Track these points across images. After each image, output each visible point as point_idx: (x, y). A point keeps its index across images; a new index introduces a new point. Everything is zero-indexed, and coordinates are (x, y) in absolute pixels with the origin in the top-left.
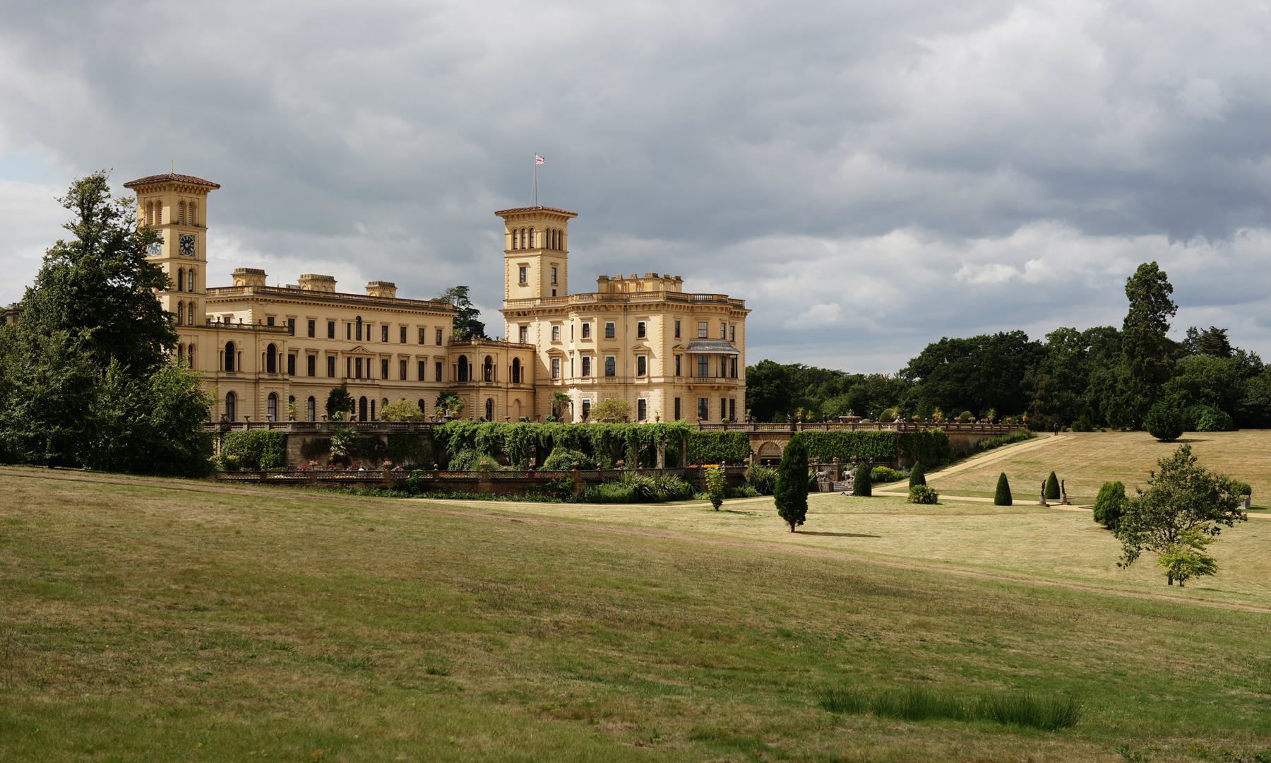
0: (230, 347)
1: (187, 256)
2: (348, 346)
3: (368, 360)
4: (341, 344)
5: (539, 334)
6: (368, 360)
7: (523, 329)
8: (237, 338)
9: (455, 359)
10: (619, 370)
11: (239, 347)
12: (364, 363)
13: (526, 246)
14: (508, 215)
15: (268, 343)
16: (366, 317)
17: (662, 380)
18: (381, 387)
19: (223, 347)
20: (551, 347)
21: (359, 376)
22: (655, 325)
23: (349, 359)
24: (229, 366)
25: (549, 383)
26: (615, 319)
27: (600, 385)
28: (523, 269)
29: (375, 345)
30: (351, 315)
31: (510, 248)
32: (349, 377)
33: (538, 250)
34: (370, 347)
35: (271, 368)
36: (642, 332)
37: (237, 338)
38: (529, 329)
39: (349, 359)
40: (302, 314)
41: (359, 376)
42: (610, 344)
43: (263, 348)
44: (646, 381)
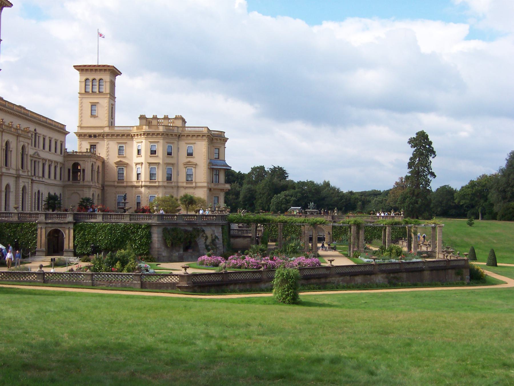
5: (107, 150)
7: (93, 146)
9: (70, 165)
10: (174, 178)
13: (96, 90)
14: (82, 69)
17: (205, 184)
20: (119, 160)
22: (201, 149)
25: (116, 184)
26: (173, 143)
27: (165, 187)
28: (93, 105)
31: (83, 92)
33: (107, 94)
36: (190, 155)
38: (98, 146)
42: (170, 160)
44: (194, 185)
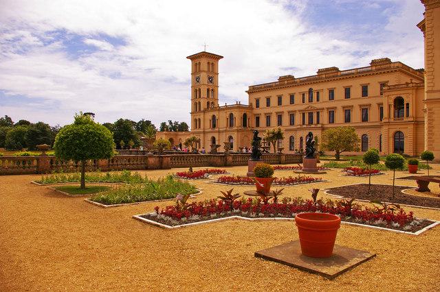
0: (214, 116)
1: (211, 84)
2: (303, 107)
3: (318, 113)
4: (299, 106)
6: (318, 113)
8: (216, 114)
11: (217, 117)
12: (315, 116)
15: (229, 113)
16: (315, 88)
18: (323, 129)
19: (210, 118)
21: (311, 122)
23: (304, 114)
24: (214, 126)
29: (324, 103)
30: (306, 89)
32: (304, 124)
34: (318, 106)
35: (231, 125)
37: (216, 114)
39: (304, 114)
40: (274, 95)
41: (311, 122)
43: (228, 116)
